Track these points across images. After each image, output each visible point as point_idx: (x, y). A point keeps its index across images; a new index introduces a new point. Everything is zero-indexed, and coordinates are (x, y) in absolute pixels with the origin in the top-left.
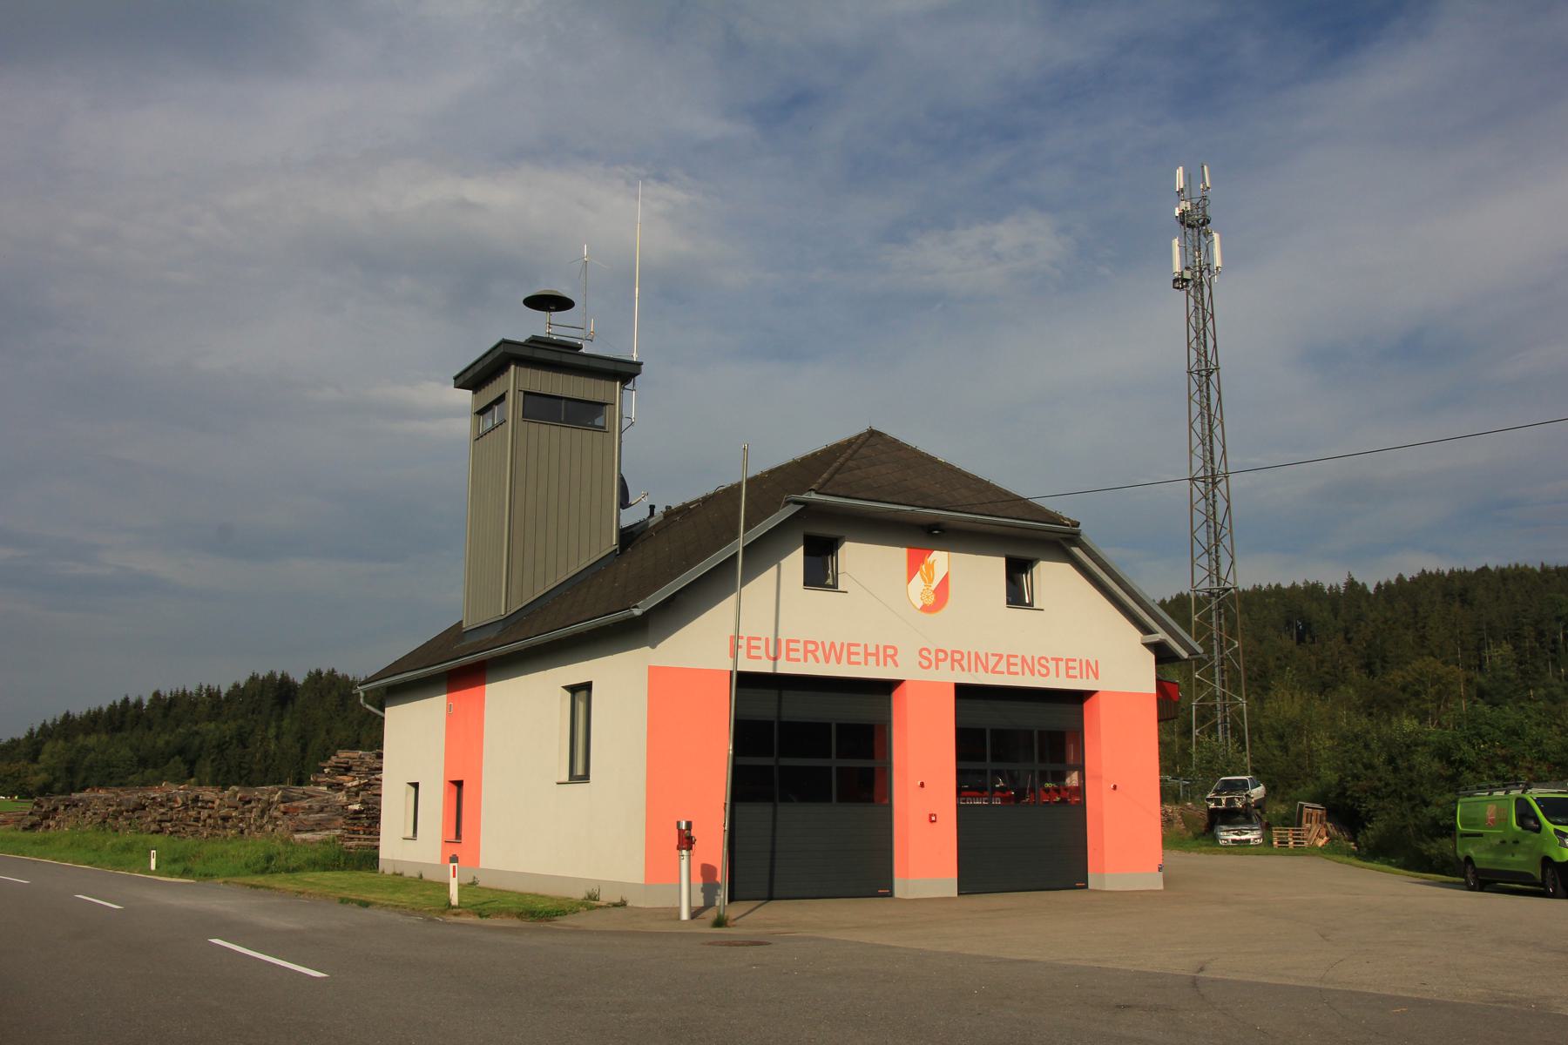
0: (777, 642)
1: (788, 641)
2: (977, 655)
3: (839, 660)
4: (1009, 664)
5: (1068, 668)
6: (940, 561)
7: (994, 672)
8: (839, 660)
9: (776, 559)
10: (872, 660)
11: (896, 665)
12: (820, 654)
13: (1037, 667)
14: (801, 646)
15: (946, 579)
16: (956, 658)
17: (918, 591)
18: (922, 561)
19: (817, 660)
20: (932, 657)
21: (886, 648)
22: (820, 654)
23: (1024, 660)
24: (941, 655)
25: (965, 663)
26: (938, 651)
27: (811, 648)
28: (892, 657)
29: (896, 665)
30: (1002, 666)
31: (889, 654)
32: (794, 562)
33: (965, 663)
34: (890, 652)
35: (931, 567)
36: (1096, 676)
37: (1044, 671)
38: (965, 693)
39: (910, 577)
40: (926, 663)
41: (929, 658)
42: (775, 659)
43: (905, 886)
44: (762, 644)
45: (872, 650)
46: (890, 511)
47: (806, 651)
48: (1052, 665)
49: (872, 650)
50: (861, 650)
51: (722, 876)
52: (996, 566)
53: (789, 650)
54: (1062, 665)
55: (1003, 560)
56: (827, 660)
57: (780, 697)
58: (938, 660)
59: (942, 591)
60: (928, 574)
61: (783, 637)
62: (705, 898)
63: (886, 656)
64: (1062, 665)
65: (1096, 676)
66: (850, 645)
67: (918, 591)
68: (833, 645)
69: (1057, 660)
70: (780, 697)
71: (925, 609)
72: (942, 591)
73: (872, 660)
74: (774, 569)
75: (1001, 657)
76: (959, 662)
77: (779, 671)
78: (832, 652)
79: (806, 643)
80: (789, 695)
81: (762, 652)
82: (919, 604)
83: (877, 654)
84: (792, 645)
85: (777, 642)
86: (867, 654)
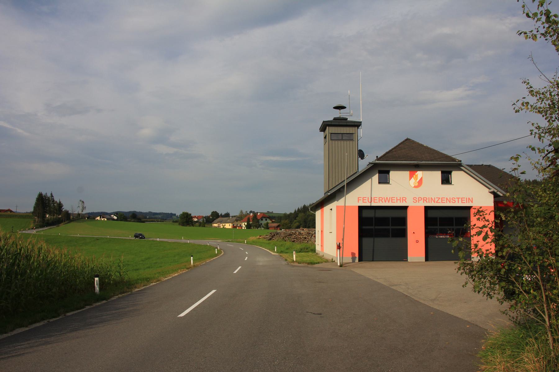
0: (371, 198)
3: (389, 202)
5: (462, 200)
6: (420, 174)
8: (389, 202)
9: (371, 177)
10: (399, 201)
12: (383, 200)
14: (378, 199)
15: (421, 179)
16: (425, 199)
17: (413, 182)
20: (417, 199)
22: (383, 200)
23: (447, 199)
27: (380, 199)
30: (440, 201)
31: (404, 199)
32: (376, 178)
35: (417, 176)
36: (472, 202)
39: (410, 179)
44: (367, 199)
45: (399, 198)
48: (456, 200)
49: (399, 198)
50: (395, 199)
51: (357, 255)
52: (437, 175)
54: (460, 200)
56: (385, 202)
58: (419, 200)
59: (420, 182)
61: (373, 197)
64: (460, 200)
65: (472, 202)
67: (413, 182)
69: (458, 198)
71: (415, 187)
72: (420, 182)
73: (399, 201)
74: (370, 180)
75: (439, 198)
77: (372, 205)
78: (387, 199)
80: (377, 211)
81: (367, 201)
82: (413, 186)
83: (400, 200)
85: (371, 198)
86: (397, 200)
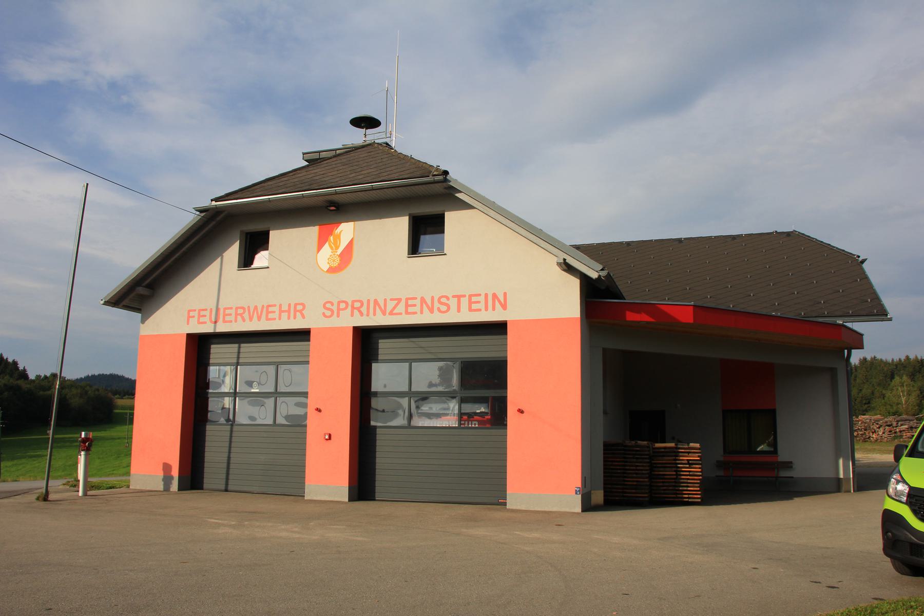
0: (218, 309)
1: (225, 309)
2: (376, 302)
3: (259, 318)
4: (407, 306)
5: (470, 303)
6: (346, 230)
7: (391, 313)
8: (259, 318)
9: (220, 254)
10: (285, 315)
11: (303, 317)
12: (246, 315)
13: (436, 305)
14: (233, 312)
15: (350, 245)
16: (356, 307)
17: (326, 256)
18: (331, 233)
19: (244, 320)
20: (335, 308)
21: (296, 305)
22: (246, 315)
23: (423, 300)
24: (343, 306)
25: (364, 309)
26: (339, 303)
27: (241, 311)
28: (301, 311)
29: (303, 317)
30: (401, 308)
31: (299, 309)
32: (233, 253)
33: (364, 309)
34: (299, 307)
35: (339, 236)
36: (504, 307)
37: (444, 308)
38: (188, 335)
39: (320, 246)
40: (328, 313)
41: (330, 309)
42: (215, 322)
43: (519, 496)
44: (207, 313)
45: (285, 308)
46: (270, 201)
47: (237, 314)
48: (453, 303)
49: (285, 308)
50: (276, 309)
51: (175, 473)
52: (398, 227)
53: (225, 315)
54: (465, 302)
55: (407, 218)
56: (251, 319)
57: (239, 347)
58: (339, 309)
59: (347, 255)
60: (335, 243)
61: (221, 307)
62: (165, 485)
63: (296, 311)
64: (465, 302)
65: (504, 307)
66: (268, 306)
67: (326, 256)
68: (256, 308)
69: (459, 297)
70: (239, 347)
71: (331, 270)
72: (347, 255)
73: (285, 315)
74: (219, 260)
75: (399, 300)
76: (358, 309)
77: (218, 330)
78: (255, 312)
79: (237, 308)
80: (247, 348)
81: (207, 319)
82: (325, 267)
83: (289, 311)
84: (228, 312)
85: (218, 309)
86: (281, 311)
